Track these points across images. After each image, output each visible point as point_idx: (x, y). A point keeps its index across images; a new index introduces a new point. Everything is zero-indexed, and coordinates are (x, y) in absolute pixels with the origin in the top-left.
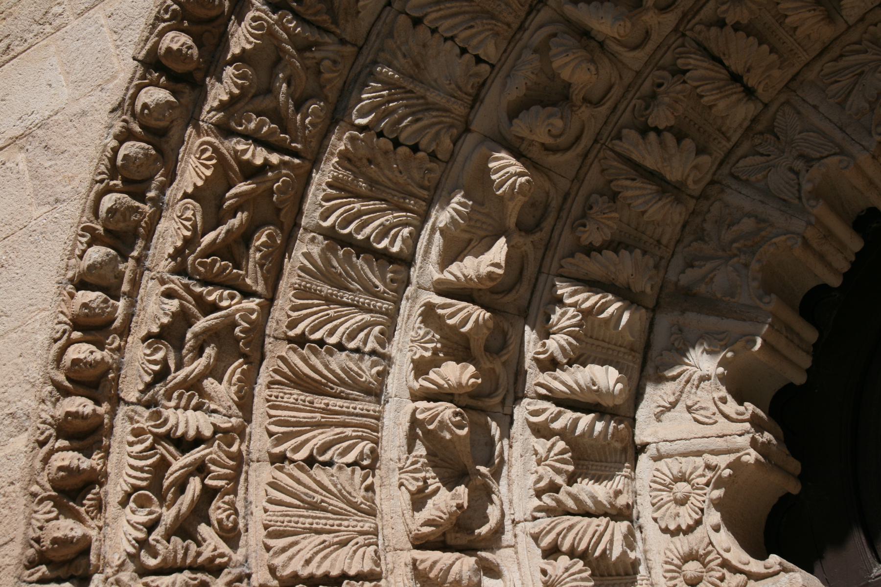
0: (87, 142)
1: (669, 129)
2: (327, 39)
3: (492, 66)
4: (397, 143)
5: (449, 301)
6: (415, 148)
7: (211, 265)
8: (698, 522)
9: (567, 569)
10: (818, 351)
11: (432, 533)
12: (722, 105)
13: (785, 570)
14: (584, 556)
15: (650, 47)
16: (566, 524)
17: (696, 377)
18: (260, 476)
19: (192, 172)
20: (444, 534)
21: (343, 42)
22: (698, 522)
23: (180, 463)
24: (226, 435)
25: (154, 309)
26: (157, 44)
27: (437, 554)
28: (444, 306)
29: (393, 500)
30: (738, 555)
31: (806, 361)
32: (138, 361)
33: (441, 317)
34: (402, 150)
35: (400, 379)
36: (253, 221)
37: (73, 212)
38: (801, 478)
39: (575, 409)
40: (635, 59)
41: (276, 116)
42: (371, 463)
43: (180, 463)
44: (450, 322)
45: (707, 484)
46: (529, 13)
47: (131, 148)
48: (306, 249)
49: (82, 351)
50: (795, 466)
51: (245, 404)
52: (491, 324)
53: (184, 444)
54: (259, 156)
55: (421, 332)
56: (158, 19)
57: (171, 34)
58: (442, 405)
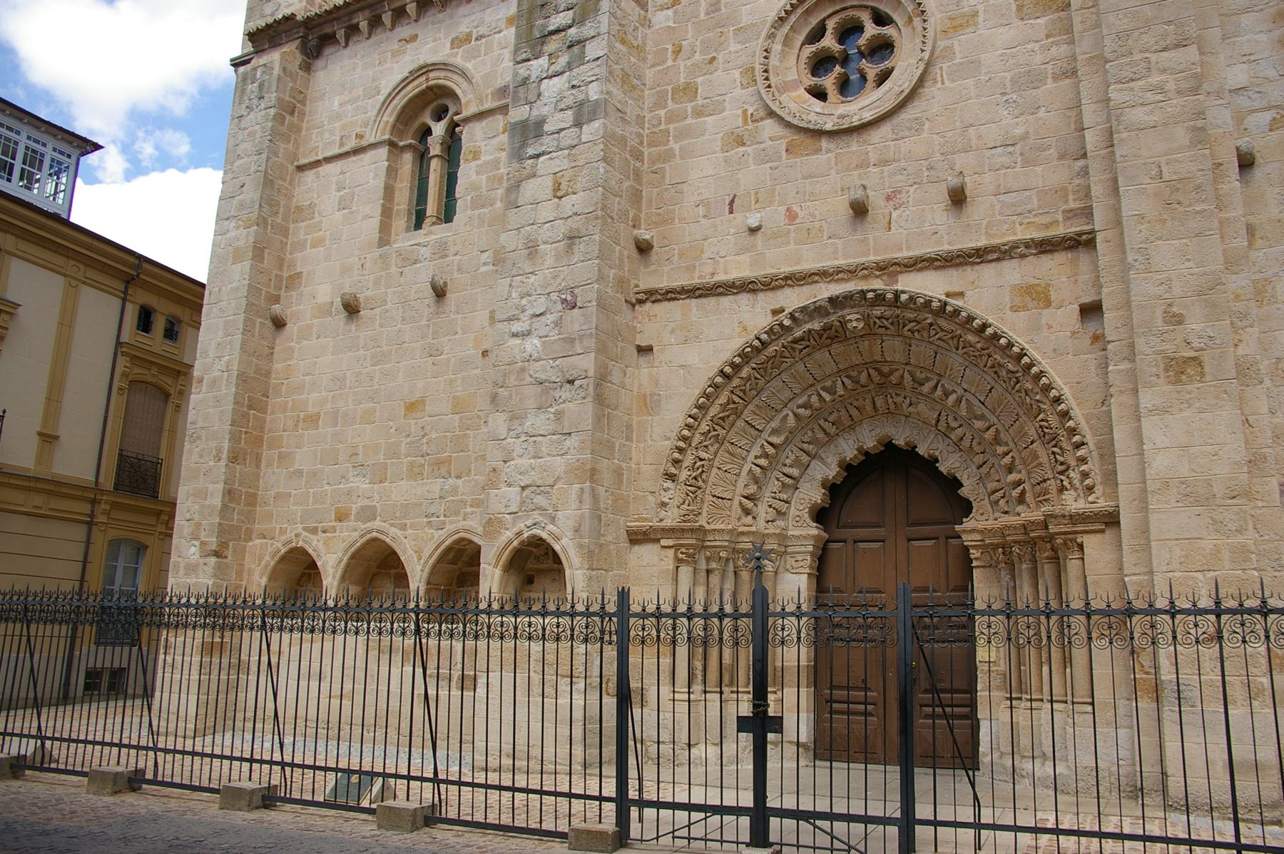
0: (699, 383)
7: (720, 421)
18: (715, 470)
19: (723, 399)
23: (699, 463)
24: (710, 460)
25: (704, 427)
29: (741, 484)
30: (808, 520)
32: (697, 439)
35: (751, 458)
36: (733, 412)
37: (693, 400)
42: (738, 475)
43: (699, 463)
47: (710, 389)
48: (740, 423)
49: (686, 432)
51: (716, 453)
53: (701, 460)
54: (736, 399)
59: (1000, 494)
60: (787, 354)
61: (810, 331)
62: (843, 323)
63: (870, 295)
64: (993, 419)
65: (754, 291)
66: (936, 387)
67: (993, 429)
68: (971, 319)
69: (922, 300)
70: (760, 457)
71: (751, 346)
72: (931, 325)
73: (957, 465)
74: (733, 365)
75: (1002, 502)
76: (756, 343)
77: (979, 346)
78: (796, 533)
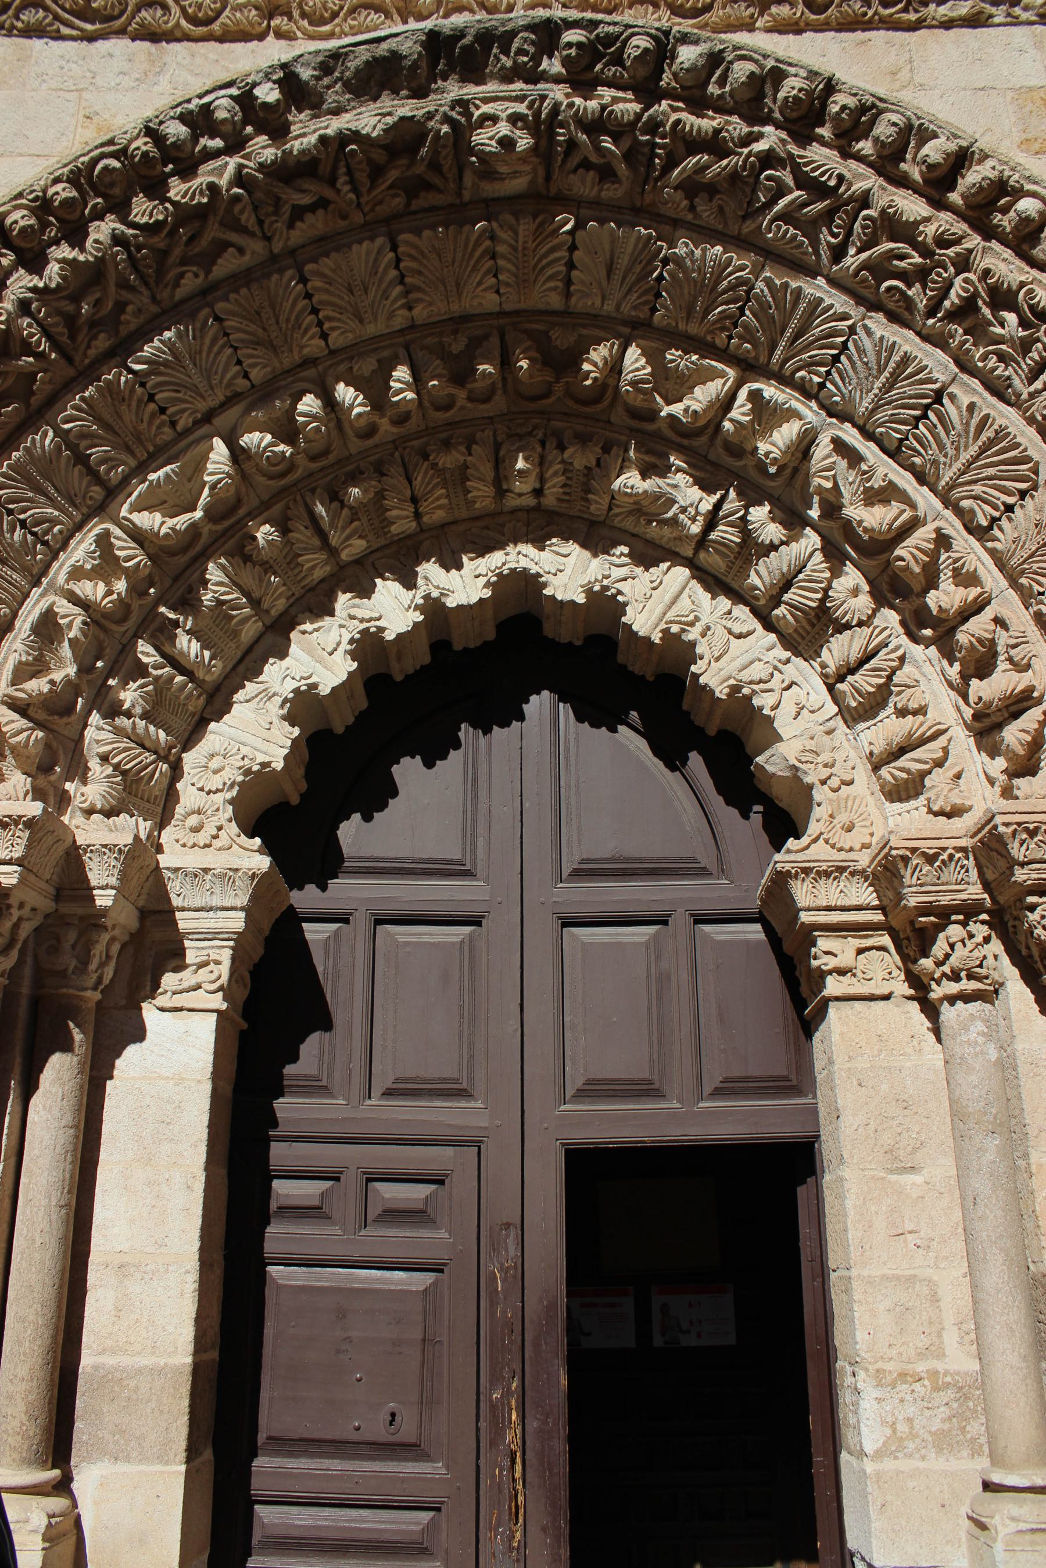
1: (351, 508)
2: (143, 289)
3: (253, 386)
4: (151, 398)
5: (125, 536)
6: (163, 410)
8: (218, 791)
9: (108, 776)
10: (361, 717)
11: (21, 699)
12: (395, 513)
13: (260, 851)
14: (124, 773)
15: (370, 442)
16: (123, 745)
17: (272, 691)
20: (29, 705)
21: (154, 299)
22: (218, 791)
26: (9, 213)
27: (16, 716)
28: (118, 538)
31: (351, 720)
33: (112, 545)
34: (152, 406)
38: (302, 796)
39: (174, 668)
40: (356, 445)
41: (71, 321)
44: (118, 553)
45: (240, 768)
46: (300, 366)
50: (304, 786)
52: (147, 571)
55: (93, 548)
56: (20, 195)
57: (25, 212)
58: (77, 610)
59: (930, 751)
60: (248, 218)
61: (345, 138)
62: (463, 122)
63: (572, 36)
64: (925, 499)
65: (154, 36)
66: (727, 402)
67: (923, 536)
68: (914, 132)
69: (750, 67)
70: (95, 574)
71: (121, 154)
72: (768, 159)
73: (758, 671)
74: (42, 206)
75: (937, 780)
76: (142, 144)
77: (930, 230)
78: (192, 860)
